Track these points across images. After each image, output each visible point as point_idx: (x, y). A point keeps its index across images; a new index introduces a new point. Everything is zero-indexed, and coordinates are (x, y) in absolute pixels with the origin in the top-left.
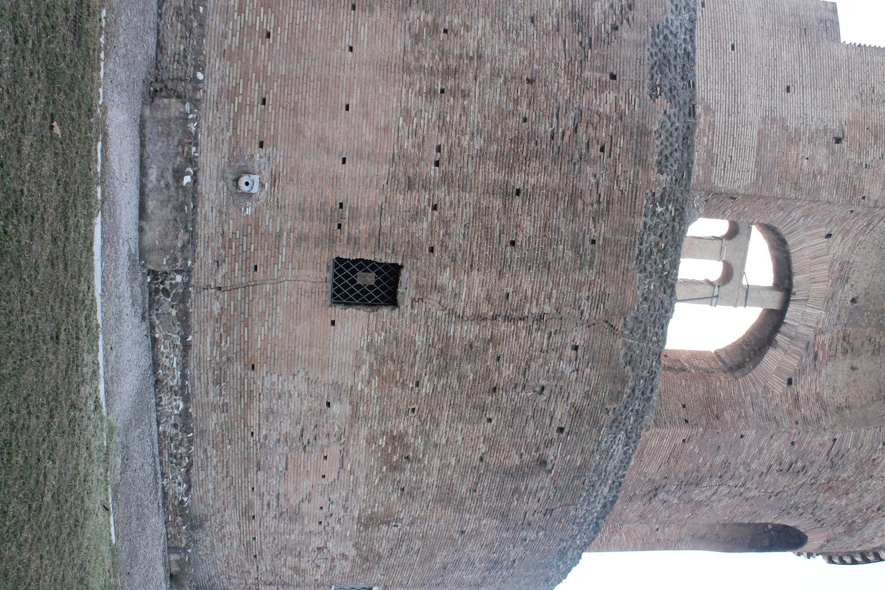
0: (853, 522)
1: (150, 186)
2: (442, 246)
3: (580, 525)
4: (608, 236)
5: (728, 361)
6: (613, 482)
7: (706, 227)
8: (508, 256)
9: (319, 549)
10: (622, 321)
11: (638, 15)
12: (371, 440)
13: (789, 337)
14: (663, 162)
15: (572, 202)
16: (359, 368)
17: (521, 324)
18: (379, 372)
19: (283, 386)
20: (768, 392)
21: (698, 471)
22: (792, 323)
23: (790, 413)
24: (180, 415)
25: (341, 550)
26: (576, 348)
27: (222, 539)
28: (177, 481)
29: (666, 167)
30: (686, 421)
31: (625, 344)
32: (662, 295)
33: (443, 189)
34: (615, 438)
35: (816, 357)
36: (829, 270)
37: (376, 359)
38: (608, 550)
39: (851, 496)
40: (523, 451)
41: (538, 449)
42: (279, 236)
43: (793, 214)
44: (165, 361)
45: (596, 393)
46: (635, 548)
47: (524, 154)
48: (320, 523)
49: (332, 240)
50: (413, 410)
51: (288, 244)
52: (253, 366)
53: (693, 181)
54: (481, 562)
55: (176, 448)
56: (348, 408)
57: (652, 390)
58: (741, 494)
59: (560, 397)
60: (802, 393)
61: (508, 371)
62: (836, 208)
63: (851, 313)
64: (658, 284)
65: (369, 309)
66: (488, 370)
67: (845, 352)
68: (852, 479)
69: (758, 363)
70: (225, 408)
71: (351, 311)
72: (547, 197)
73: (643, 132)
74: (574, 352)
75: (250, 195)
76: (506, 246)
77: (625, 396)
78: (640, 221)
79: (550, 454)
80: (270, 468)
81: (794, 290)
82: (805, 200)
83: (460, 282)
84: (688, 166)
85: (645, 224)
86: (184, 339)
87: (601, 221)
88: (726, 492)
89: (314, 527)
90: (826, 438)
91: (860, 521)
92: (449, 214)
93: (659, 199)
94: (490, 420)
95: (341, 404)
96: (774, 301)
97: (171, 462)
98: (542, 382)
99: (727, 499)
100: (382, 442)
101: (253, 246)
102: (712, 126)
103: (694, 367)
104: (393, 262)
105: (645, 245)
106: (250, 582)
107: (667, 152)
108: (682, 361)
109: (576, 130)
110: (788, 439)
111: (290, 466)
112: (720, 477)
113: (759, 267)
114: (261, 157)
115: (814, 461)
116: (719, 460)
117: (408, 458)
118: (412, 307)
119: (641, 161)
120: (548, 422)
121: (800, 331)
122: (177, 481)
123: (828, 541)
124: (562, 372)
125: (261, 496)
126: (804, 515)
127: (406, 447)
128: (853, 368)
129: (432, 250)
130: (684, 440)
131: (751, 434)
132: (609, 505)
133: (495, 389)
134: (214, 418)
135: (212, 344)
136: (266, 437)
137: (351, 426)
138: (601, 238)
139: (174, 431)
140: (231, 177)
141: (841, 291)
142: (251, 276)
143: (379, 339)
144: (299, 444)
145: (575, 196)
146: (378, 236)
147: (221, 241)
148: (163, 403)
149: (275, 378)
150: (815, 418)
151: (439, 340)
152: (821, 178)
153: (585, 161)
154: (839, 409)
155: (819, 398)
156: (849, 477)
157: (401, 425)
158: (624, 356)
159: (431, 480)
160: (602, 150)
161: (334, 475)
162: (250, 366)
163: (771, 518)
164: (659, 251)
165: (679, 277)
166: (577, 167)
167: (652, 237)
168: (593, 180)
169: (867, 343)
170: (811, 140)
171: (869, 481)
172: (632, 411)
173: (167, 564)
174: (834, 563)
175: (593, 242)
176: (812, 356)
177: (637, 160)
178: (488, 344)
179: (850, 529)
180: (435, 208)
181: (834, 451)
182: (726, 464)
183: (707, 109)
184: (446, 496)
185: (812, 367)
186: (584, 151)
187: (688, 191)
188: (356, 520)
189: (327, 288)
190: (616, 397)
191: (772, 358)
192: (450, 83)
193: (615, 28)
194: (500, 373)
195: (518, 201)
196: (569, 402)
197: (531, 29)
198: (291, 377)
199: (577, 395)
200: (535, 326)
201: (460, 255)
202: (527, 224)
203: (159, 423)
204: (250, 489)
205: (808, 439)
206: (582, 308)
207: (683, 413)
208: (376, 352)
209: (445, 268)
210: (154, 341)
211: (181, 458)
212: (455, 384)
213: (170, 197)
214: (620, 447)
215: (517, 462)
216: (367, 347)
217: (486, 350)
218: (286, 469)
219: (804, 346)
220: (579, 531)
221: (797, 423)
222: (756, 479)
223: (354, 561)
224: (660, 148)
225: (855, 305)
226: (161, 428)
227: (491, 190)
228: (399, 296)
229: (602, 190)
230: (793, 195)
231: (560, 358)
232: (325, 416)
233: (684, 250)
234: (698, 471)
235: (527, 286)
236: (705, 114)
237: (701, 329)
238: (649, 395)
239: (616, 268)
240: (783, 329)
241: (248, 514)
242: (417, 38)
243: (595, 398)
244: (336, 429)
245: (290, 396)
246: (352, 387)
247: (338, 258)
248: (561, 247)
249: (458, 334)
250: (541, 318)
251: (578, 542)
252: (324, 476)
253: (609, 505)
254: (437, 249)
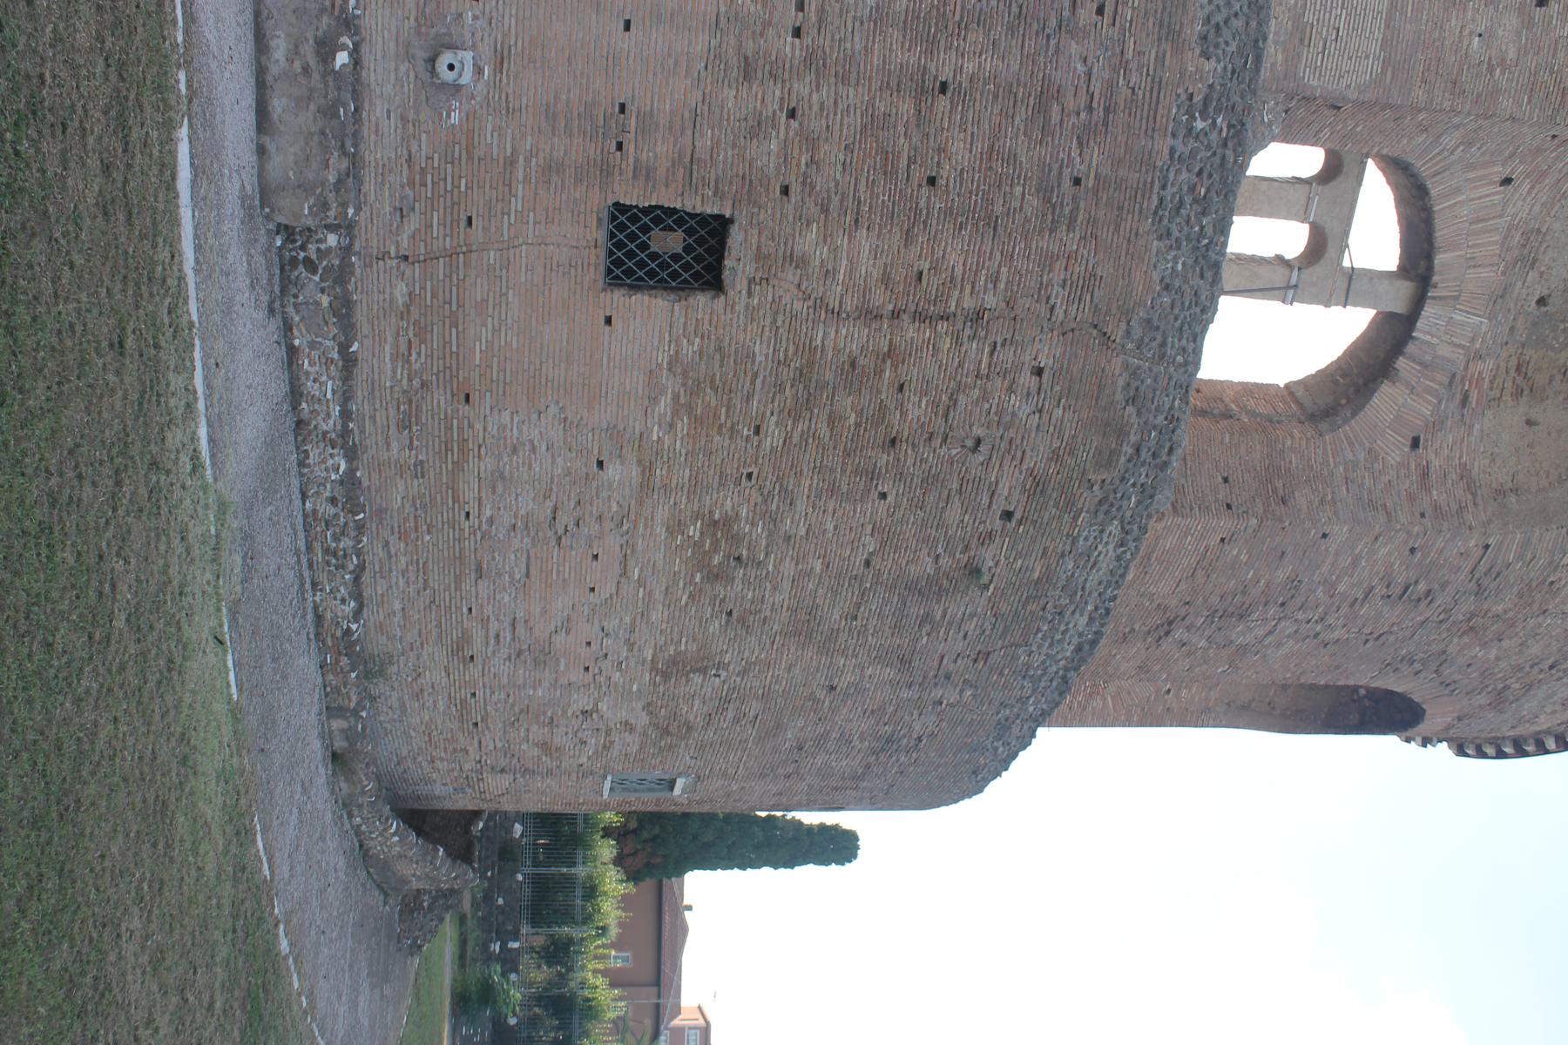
0: (1506, 688)
1: (274, 70)
2: (804, 183)
3: (1036, 680)
4: (1105, 171)
5: (1307, 402)
6: (1096, 608)
7: (1285, 160)
8: (922, 203)
9: (584, 713)
10: (1123, 326)
12: (676, 527)
13: (1420, 364)
14: (1211, 36)
15: (1041, 108)
16: (654, 400)
17: (942, 327)
18: (690, 408)
19: (520, 432)
20: (1376, 459)
21: (1243, 593)
22: (1428, 338)
23: (1411, 498)
24: (342, 482)
25: (623, 714)
26: (1039, 372)
27: (418, 696)
28: (339, 596)
29: (1217, 46)
30: (1229, 506)
31: (1126, 366)
32: (1196, 282)
33: (808, 80)
34: (1102, 532)
35: (1464, 402)
36: (1502, 244)
37: (684, 385)
38: (1082, 724)
39: (1506, 643)
40: (940, 550)
41: (966, 548)
42: (511, 163)
43: (1445, 139)
44: (311, 387)
45: (1071, 453)
46: (1128, 723)
47: (957, 18)
48: (587, 669)
49: (606, 171)
50: (749, 476)
51: (527, 179)
52: (467, 396)
53: (1265, 73)
54: (862, 739)
55: (336, 539)
56: (635, 472)
57: (1171, 450)
58: (1316, 636)
59: (1007, 462)
60: (1436, 463)
61: (918, 409)
62: (1525, 129)
63: (1535, 324)
64: (1190, 262)
65: (672, 297)
66: (882, 407)
67: (1518, 393)
68: (1511, 614)
69: (1362, 407)
70: (419, 470)
71: (640, 300)
72: (996, 97)
74: (1035, 379)
75: (456, 88)
76: (920, 185)
77: (1123, 459)
78: (1163, 145)
79: (988, 557)
80: (499, 575)
81: (1435, 278)
82: (1469, 114)
83: (835, 250)
84: (1255, 46)
85: (1172, 150)
86: (344, 348)
87: (1092, 143)
88: (1291, 630)
89: (576, 675)
90: (1472, 543)
91: (1517, 686)
92: (817, 125)
93: (1200, 106)
94: (883, 496)
95: (622, 464)
96: (1397, 301)
97: (328, 564)
98: (978, 431)
99: (1291, 642)
100: (694, 531)
101: (463, 181)
103: (1247, 412)
104: (716, 211)
105: (1170, 190)
106: (467, 766)
107: (1219, 18)
108: (1227, 400)
110: (1406, 543)
111: (533, 572)
112: (1283, 604)
113: (1375, 235)
114: (475, 18)
115: (1447, 582)
116: (1281, 575)
117: (738, 559)
118: (750, 294)
119: (1170, 34)
120: (985, 500)
121: (1440, 353)
122: (339, 596)
123: (1459, 719)
124: (1014, 414)
125: (485, 622)
126: (1423, 675)
127: (736, 539)
128: (1529, 423)
129: (785, 191)
130: (1223, 540)
131: (1340, 532)
132: (1087, 647)
133: (893, 441)
134: (401, 485)
135: (394, 358)
136: (491, 521)
137: (640, 504)
138: (1092, 175)
139: (331, 510)
140: (421, 54)
141: (1519, 284)
142: (462, 236)
143: (689, 350)
144: (549, 534)
145: (1047, 95)
146: (690, 164)
147: (405, 172)
148: (311, 461)
149: (506, 417)
150: (1454, 507)
151: (796, 353)
152: (1502, 72)
153: (1067, 32)
154: (1500, 493)
155: (1465, 473)
156: (1505, 612)
157: (727, 502)
158: (1124, 389)
159: (778, 598)
160: (1100, 11)
161: (610, 588)
162: (463, 397)
163: (1366, 677)
164: (1195, 201)
165: (1229, 250)
166: (1052, 42)
167: (1184, 175)
168: (1080, 68)
169: (1559, 377)
171: (1540, 619)
172: (1134, 485)
173: (326, 736)
174: (1468, 755)
175: (1077, 182)
176: (1459, 397)
177: (1163, 32)
178: (884, 361)
179: (1500, 700)
180: (792, 114)
181: (1482, 568)
182: (1294, 583)
184: (805, 627)
185: (1457, 417)
186: (1066, 13)
187: (1254, 93)
188: (648, 665)
189: (598, 257)
190: (1106, 459)
191: (1387, 400)
194: (904, 414)
195: (943, 102)
196: (1024, 467)
198: (535, 416)
199: (1037, 459)
200: (968, 332)
201: (836, 200)
202: (958, 146)
203: (304, 497)
204: (465, 610)
205: (1439, 544)
206: (1052, 301)
207: (1223, 492)
208: (685, 374)
209: (809, 224)
210: (292, 352)
211: (345, 556)
212: (824, 431)
213: (311, 90)
214: (1111, 547)
215: (930, 570)
216: (669, 363)
217: (879, 373)
218: (528, 576)
219: (1446, 381)
220: (1034, 690)
221: (1423, 515)
222: (1345, 609)
223: (644, 734)
224: (1207, 10)
225: (1544, 309)
226: (308, 505)
227: (893, 84)
228: (726, 274)
229: (1096, 86)
230: (1447, 104)
231: (1010, 390)
232: (594, 484)
233: (1240, 201)
234: (1243, 593)
235: (954, 259)
237: (1263, 344)
238: (1164, 458)
239: (1117, 229)
240: (1410, 348)
241: (461, 652)
243: (1069, 460)
244: (615, 508)
245: (534, 449)
246: (641, 434)
247: (617, 204)
248: (1018, 190)
249: (829, 343)
250: (978, 316)
251: (1031, 709)
252: (593, 590)
253: (1087, 647)
254: (795, 189)
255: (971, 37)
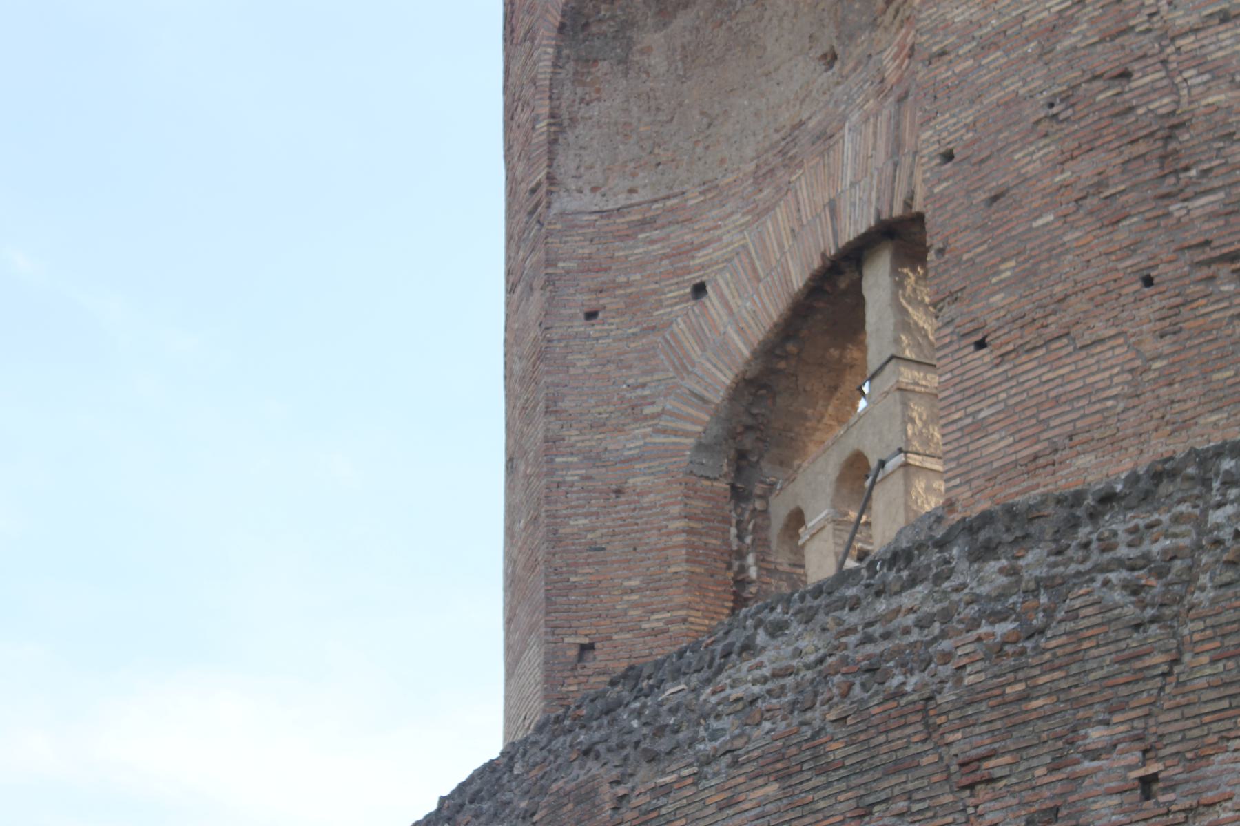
36: (776, 204)
81: (817, 264)
116: (1032, 158)
130: (981, 345)
253: (983, 536)
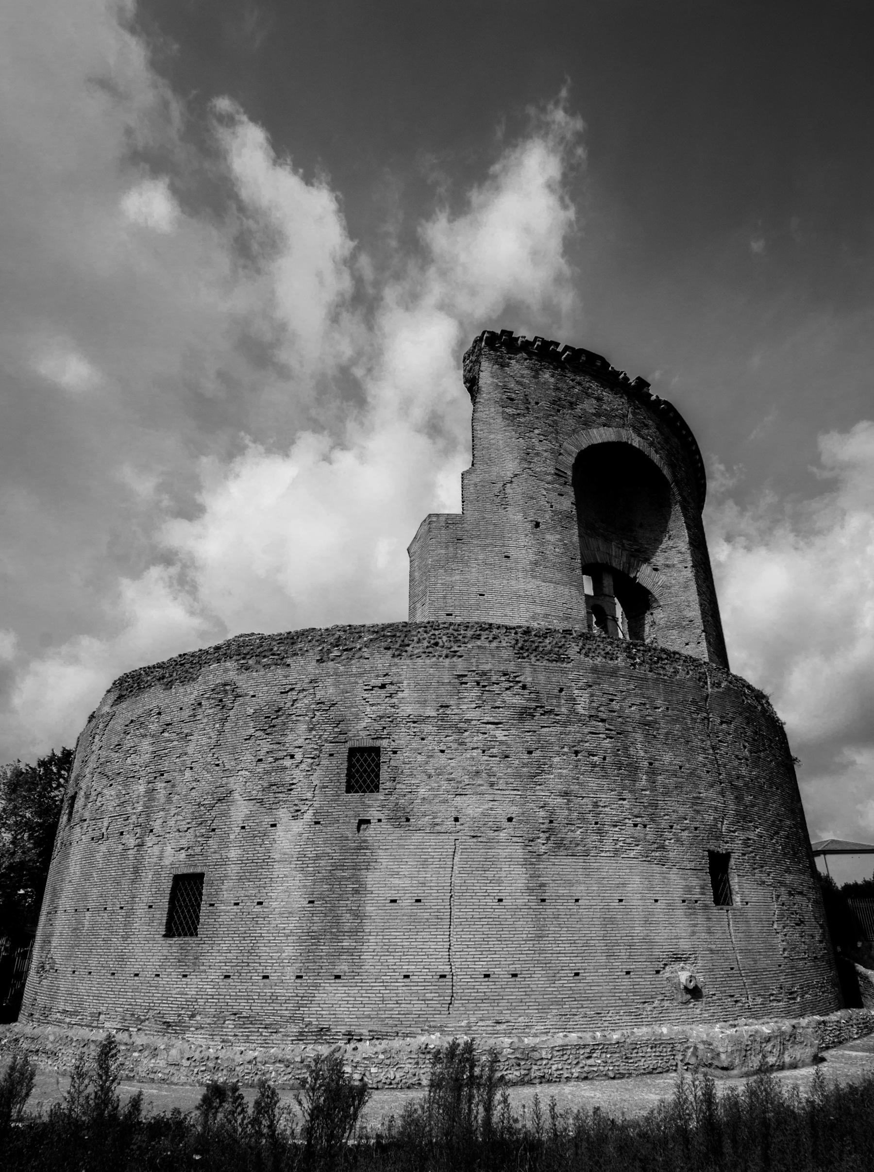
11: (511, 667)
73: (594, 670)
102: (546, 616)
109: (603, 721)
119: (614, 673)
170: (542, 544)
183: (534, 618)
192: (590, 816)
193: (524, 687)
195: (656, 764)
197: (537, 754)
236: (538, 619)
239: (678, 692)
242: (560, 845)
255: (632, 753)
